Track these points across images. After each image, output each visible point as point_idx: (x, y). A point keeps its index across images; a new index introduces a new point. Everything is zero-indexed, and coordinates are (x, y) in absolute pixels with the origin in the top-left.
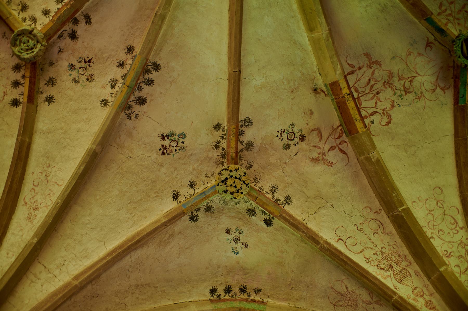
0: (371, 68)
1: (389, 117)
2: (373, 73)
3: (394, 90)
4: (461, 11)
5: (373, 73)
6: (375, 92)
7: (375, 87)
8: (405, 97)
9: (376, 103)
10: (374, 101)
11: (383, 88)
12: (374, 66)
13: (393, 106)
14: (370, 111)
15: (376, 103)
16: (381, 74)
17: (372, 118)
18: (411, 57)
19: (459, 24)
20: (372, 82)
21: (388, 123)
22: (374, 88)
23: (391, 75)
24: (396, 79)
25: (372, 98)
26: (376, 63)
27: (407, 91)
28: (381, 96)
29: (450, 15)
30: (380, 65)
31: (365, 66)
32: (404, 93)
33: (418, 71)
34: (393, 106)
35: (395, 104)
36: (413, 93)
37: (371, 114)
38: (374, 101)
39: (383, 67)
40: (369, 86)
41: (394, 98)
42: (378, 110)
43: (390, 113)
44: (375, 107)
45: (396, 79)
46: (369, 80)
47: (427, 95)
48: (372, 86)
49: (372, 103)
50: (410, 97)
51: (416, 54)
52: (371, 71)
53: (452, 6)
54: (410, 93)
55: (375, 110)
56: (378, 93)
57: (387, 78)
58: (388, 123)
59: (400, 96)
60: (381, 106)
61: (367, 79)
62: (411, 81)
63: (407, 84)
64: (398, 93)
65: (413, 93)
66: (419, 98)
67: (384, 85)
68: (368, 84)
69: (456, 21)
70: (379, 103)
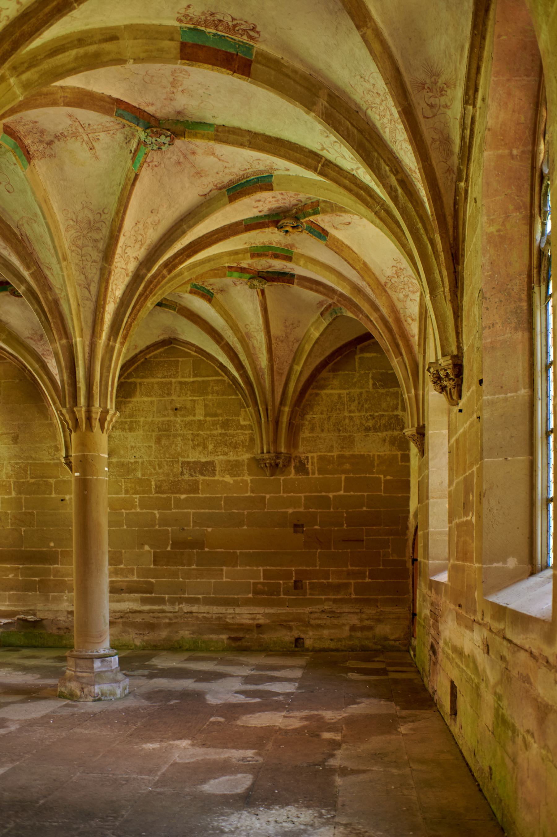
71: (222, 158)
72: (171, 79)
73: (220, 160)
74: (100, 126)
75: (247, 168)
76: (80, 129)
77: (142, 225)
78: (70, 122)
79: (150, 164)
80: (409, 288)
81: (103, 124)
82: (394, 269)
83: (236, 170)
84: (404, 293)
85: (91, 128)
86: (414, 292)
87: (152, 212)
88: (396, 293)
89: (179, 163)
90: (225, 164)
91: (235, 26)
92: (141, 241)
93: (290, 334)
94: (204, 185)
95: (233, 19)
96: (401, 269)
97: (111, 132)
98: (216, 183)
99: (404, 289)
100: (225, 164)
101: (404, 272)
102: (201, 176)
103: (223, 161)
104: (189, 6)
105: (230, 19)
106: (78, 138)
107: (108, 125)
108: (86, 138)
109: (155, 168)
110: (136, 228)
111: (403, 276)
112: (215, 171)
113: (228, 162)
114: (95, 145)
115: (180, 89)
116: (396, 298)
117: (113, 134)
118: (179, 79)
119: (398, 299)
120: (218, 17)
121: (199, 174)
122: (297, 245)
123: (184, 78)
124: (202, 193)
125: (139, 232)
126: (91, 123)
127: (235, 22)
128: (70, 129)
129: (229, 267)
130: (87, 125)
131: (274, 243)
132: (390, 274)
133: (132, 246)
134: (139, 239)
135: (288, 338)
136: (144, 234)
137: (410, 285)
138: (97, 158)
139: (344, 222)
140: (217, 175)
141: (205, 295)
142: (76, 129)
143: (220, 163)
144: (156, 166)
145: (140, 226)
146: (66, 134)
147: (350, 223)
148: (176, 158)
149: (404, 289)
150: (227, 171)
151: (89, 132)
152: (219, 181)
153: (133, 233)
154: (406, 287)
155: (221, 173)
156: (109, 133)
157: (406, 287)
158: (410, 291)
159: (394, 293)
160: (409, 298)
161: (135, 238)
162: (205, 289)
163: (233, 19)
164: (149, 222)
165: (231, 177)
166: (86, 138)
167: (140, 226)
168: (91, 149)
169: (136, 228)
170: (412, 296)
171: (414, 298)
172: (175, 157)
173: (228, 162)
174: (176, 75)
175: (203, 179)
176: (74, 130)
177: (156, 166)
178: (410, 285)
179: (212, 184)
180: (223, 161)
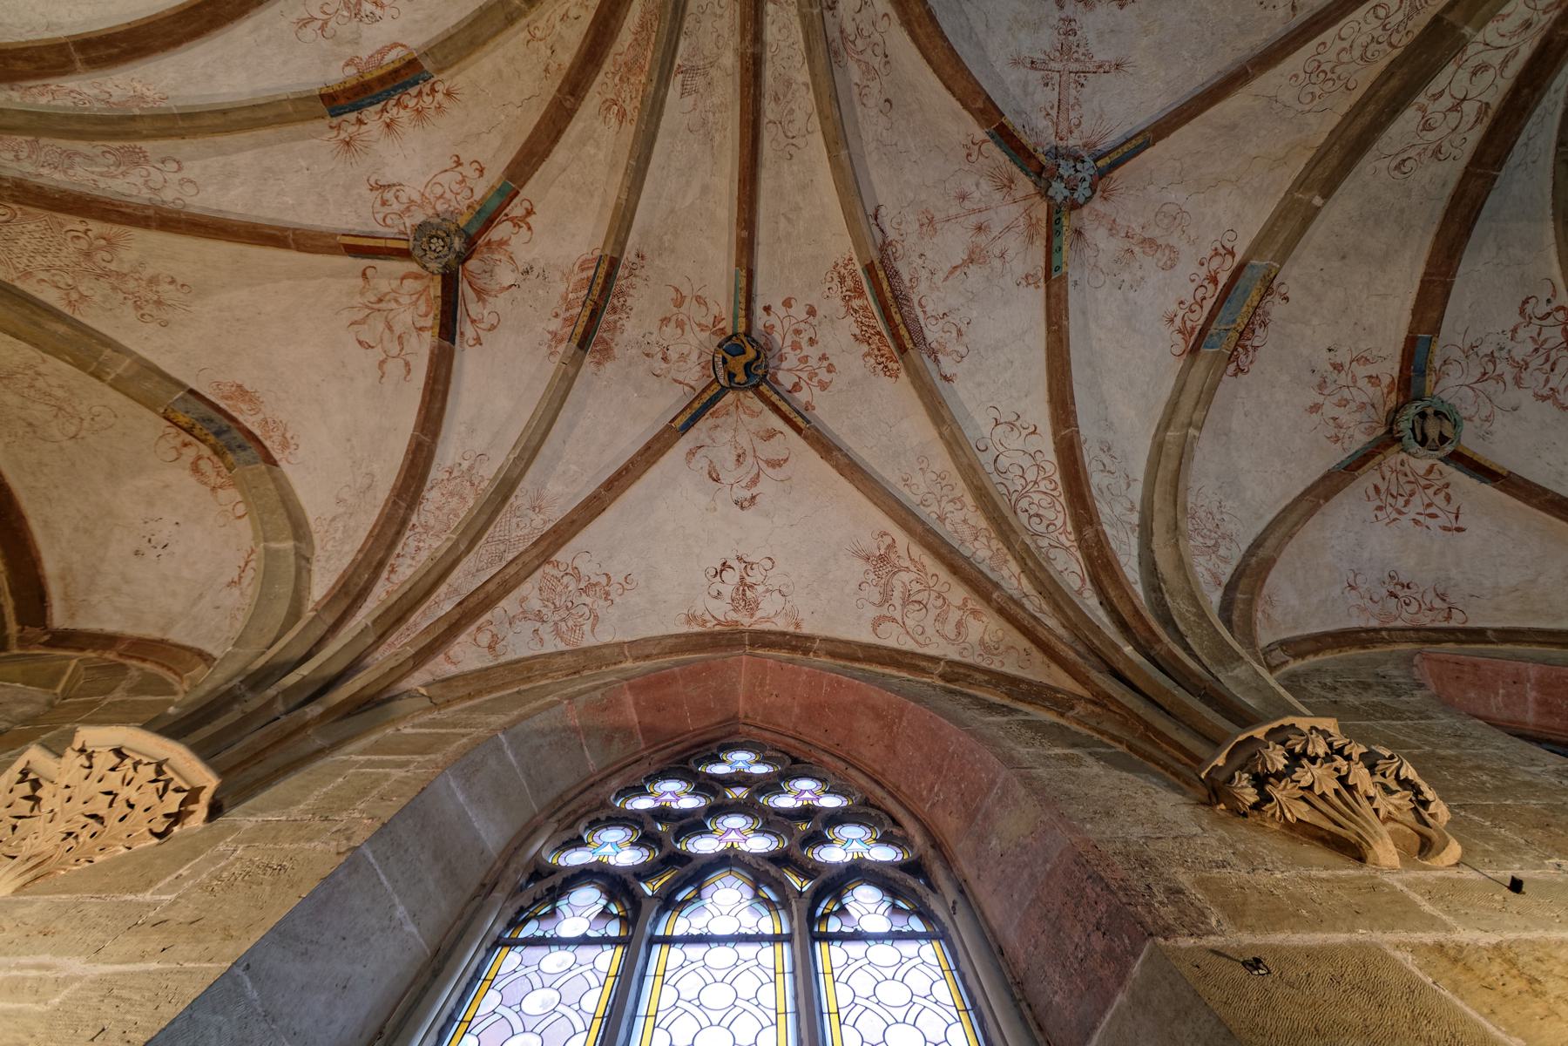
0: (1552, 389)
1: (1522, 312)
2: (1547, 381)
3: (1510, 359)
4: (1411, 496)
5: (1547, 381)
6: (1541, 351)
7: (1542, 359)
8: (1493, 347)
9: (1539, 334)
10: (1542, 338)
11: (1529, 359)
12: (1546, 392)
13: (1515, 331)
14: (1550, 321)
15: (1539, 334)
16: (1533, 379)
17: (1548, 309)
18: (1485, 412)
19: (1406, 475)
20: (1547, 367)
21: (1526, 302)
22: (1543, 357)
23: (1518, 381)
24: (1508, 378)
25: (1545, 341)
26: (1544, 398)
27: (1492, 358)
28: (1531, 347)
29: (1426, 487)
30: (1536, 395)
31: (1562, 392)
32: (1496, 354)
33: (1471, 393)
34: (1515, 331)
35: (1509, 335)
36: (1481, 354)
37: (1549, 314)
38: (1542, 338)
39: (1530, 392)
40: (1551, 360)
41: (1509, 345)
42: (1538, 322)
43: (1518, 319)
44: (1541, 327)
45: (1508, 378)
46: (1552, 370)
47: (1457, 354)
48: (1547, 360)
49: (1546, 333)
50: (1485, 350)
51: (1476, 419)
52: (1550, 385)
53: (1427, 501)
54: (1486, 355)
55: (1543, 323)
56: (1536, 350)
57: (1523, 375)
58: (1526, 302)
59: (1501, 349)
60: (1534, 329)
61: (1556, 371)
62: (1485, 374)
63: (1490, 367)
64: (1504, 354)
65: (1481, 354)
66: (1472, 348)
67: (1527, 364)
68: (1554, 364)
69: (1412, 479)
70: (1535, 334)
71: (958, 273)
72: (1159, 242)
73: (955, 268)
74: (1072, 101)
75: (927, 309)
76: (1074, 66)
77: (876, 67)
78: (1099, 57)
79: (977, 147)
80: (563, 620)
81: (1077, 107)
82: (604, 581)
83: (923, 287)
84: (544, 611)
85: (1073, 85)
86: (557, 633)
87: (887, 100)
88: (536, 592)
89: (963, 197)
90: (941, 275)
91: (1244, 347)
92: (853, 42)
93: (114, 289)
94: (900, 224)
95: (1255, 348)
96: (607, 594)
97: (1054, 113)
98: (899, 247)
99: (556, 609)
100: (941, 275)
101: (602, 602)
102: (922, 225)
103: (951, 273)
104: (1287, 299)
105: (1256, 344)
106: (1058, 54)
107: (1072, 115)
108: (1053, 65)
109: (965, 152)
110: (878, 50)
111: (588, 600)
112: (929, 254)
113: (946, 279)
114: (1039, 74)
115: (1137, 249)
116: (524, 594)
117: (1048, 114)
118: (1159, 254)
119: (523, 600)
120: (1259, 331)
121: (929, 223)
122: (609, 367)
123: (1159, 260)
124: (883, 211)
125: (869, 51)
126: (1085, 90)
127: (1250, 348)
128: (1081, 50)
129: (517, 193)
130: (1082, 80)
131: (612, 318)
132: (584, 570)
133: (858, 17)
134: (858, 42)
135: (98, 277)
136: (861, 57)
137: (570, 623)
138: (1016, 62)
139: (718, 468)
140: (917, 254)
141: (357, 95)
142: (1077, 60)
143: (947, 267)
144: (969, 155)
145: (877, 62)
146: (1071, 38)
147: (717, 480)
148: (975, 195)
149: (556, 609)
150: (924, 274)
151: (1064, 78)
152: (900, 251)
153: (877, 37)
154: (563, 613)
155: (920, 262)
156: (1052, 108)
157: (563, 613)
158: (556, 624)
159: (537, 586)
160: (538, 625)
161: (866, 33)
162: (371, 104)
163: (1255, 348)
164: (871, 84)
165: (906, 277)
166: (1053, 65)
167: (877, 62)
168: (1033, 62)
169: (878, 50)
170: (546, 630)
171: (545, 637)
172: (977, 195)
173: (946, 279)
174: (1167, 252)
175: (917, 226)
176: (1075, 56)
177: (969, 155)
178: (570, 623)
179: (898, 238)
180: (951, 273)
